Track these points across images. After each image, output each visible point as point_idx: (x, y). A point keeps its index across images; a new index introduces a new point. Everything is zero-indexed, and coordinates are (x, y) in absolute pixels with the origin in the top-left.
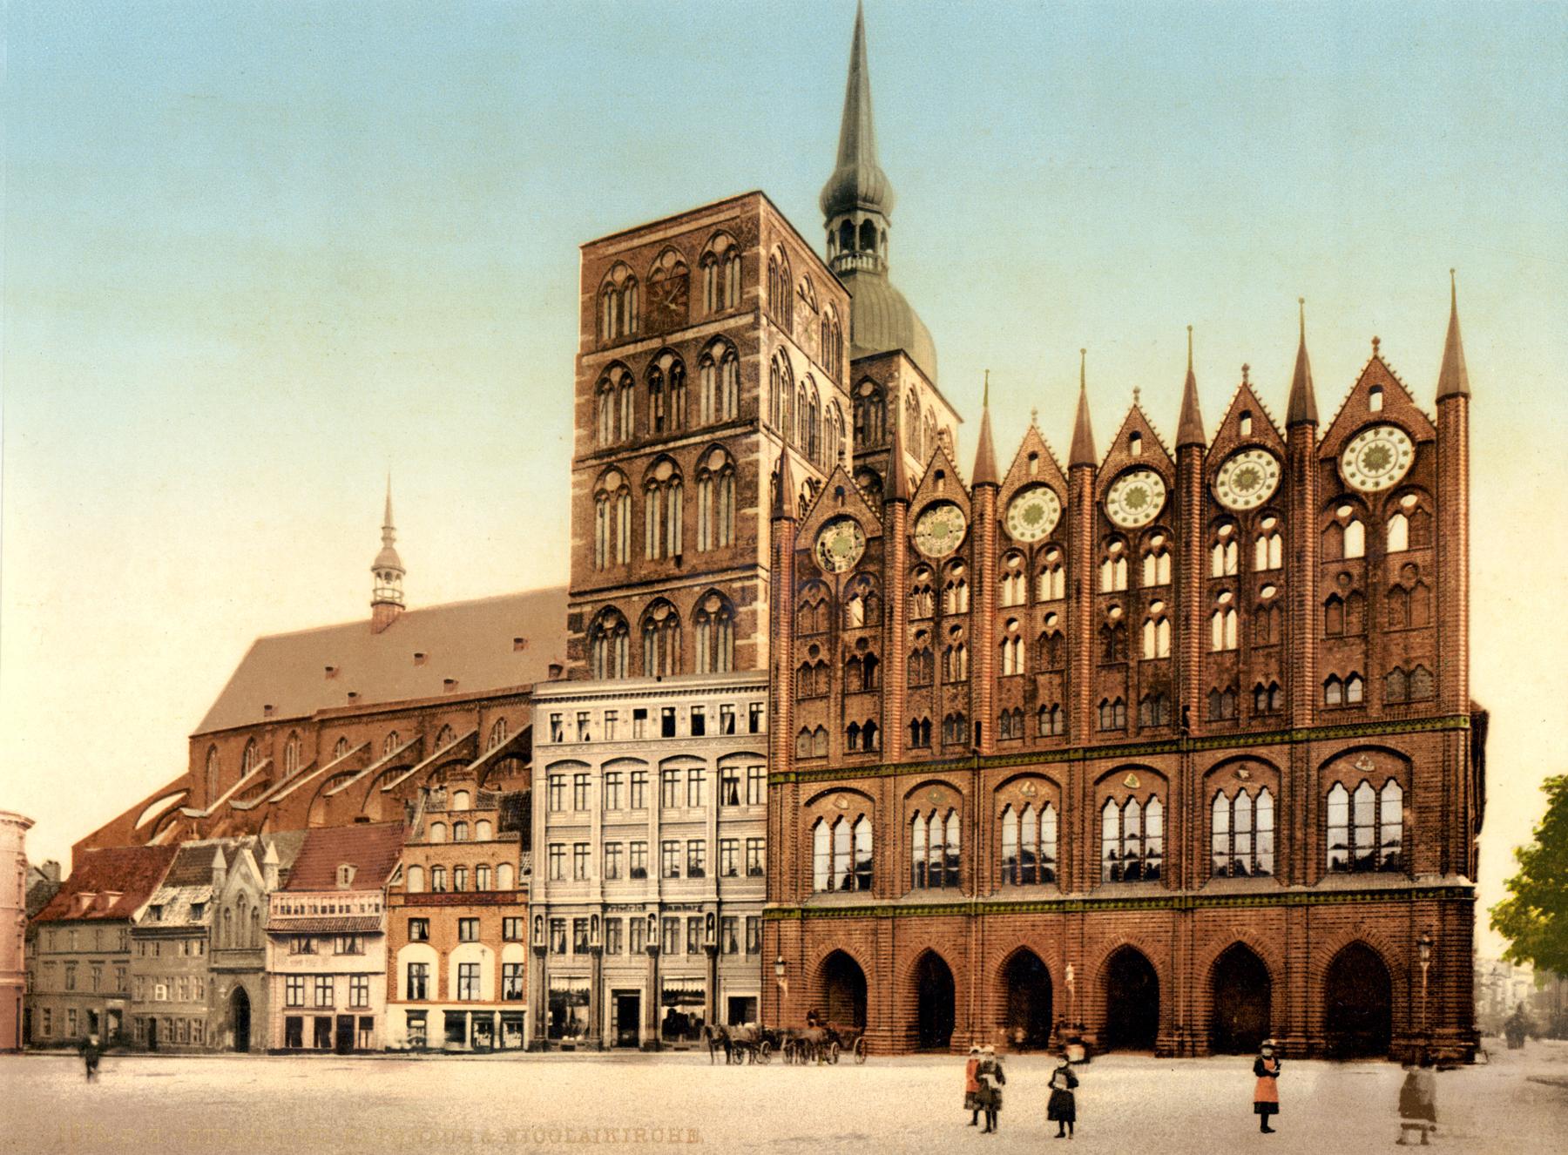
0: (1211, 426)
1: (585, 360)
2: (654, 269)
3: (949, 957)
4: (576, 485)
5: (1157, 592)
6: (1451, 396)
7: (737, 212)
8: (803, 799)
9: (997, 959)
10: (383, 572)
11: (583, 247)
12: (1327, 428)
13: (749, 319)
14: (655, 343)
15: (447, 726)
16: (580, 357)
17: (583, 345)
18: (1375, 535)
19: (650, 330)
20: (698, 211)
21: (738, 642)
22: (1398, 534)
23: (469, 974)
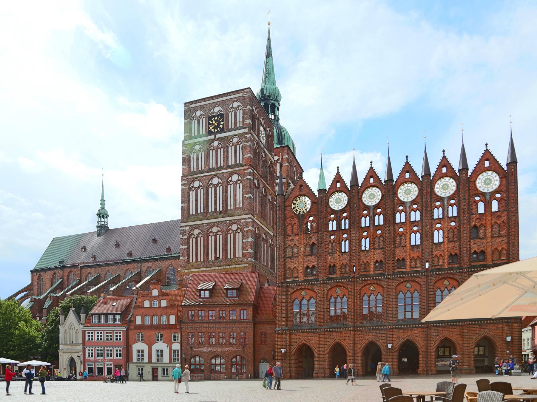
0: (433, 170)
1: (186, 142)
2: (211, 112)
3: (345, 344)
4: (182, 185)
5: (415, 223)
6: (513, 162)
7: (241, 94)
8: (290, 291)
9: (361, 346)
10: (101, 215)
11: (185, 104)
12: (472, 171)
13: (246, 130)
14: (212, 137)
15: (89, 273)
16: (183, 142)
17: (185, 136)
18: (488, 206)
20: (228, 93)
21: (244, 241)
22: (495, 206)
23: (160, 353)
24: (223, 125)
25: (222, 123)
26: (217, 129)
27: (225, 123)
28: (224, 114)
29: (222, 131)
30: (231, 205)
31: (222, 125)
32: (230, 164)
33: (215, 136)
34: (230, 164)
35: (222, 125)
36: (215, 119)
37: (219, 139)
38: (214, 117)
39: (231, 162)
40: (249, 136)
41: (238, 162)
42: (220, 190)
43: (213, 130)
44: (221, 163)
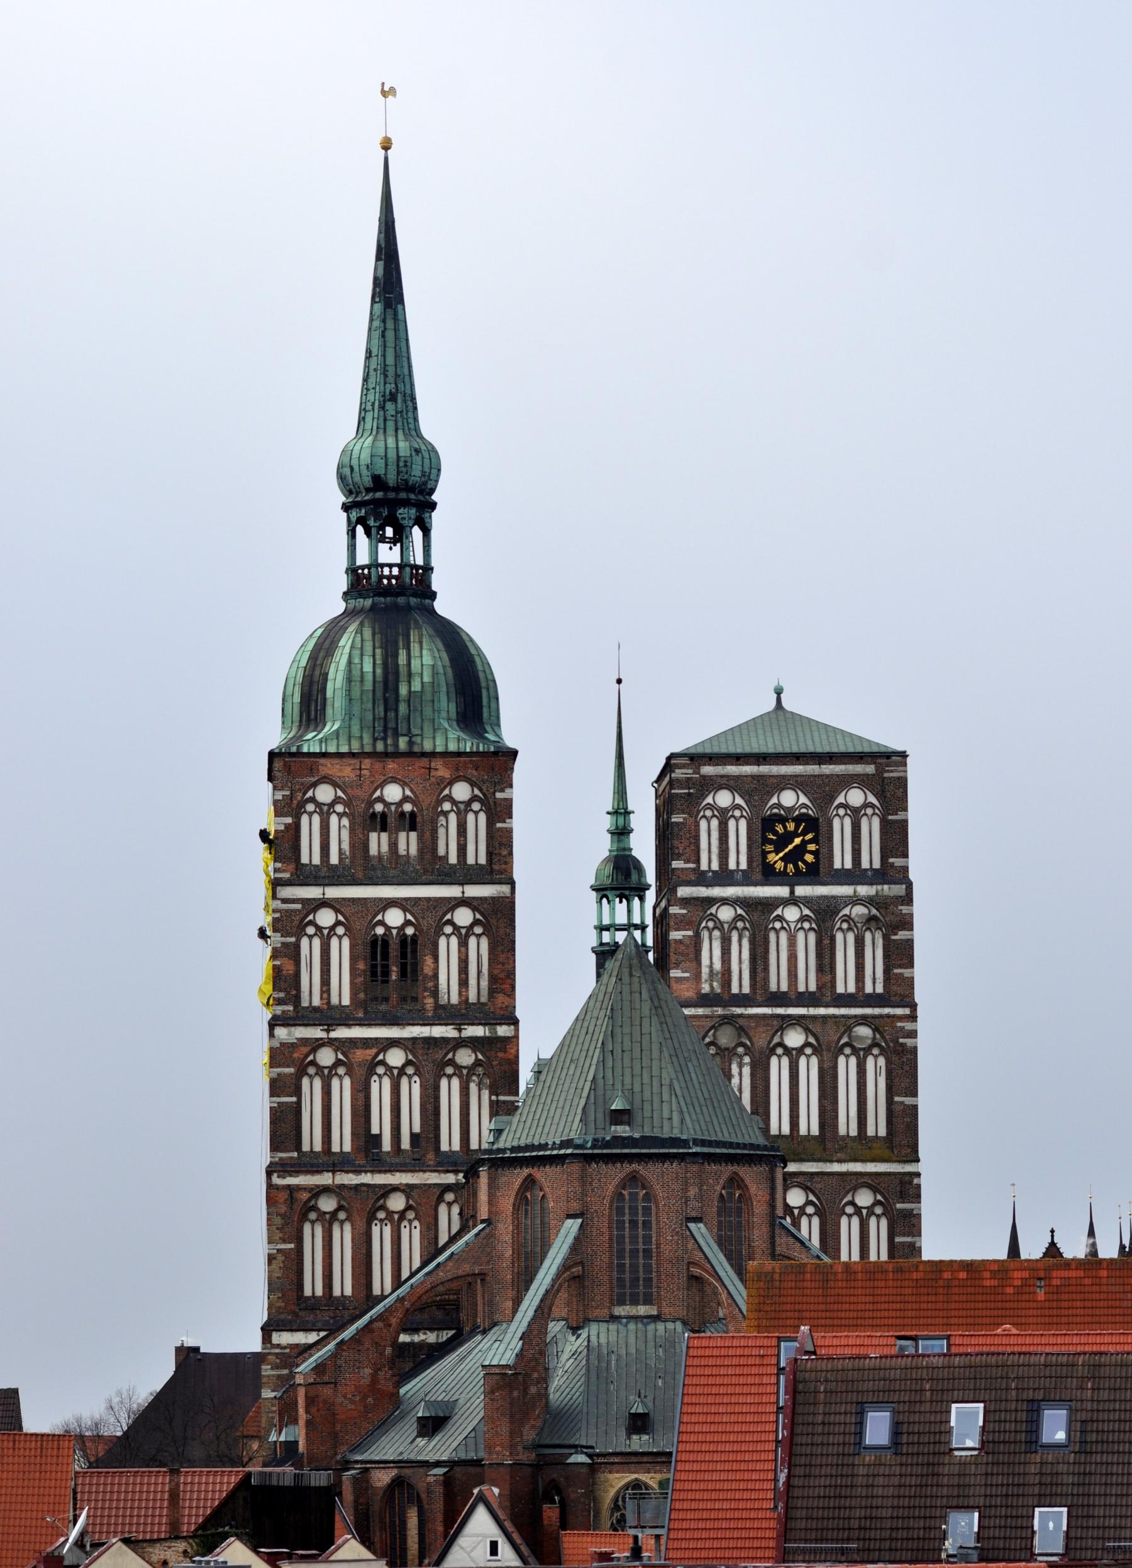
19: (769, 875)
24: (815, 853)
25: (812, 847)
26: (796, 866)
27: (824, 851)
28: (817, 819)
29: (813, 874)
30: (847, 1124)
31: (811, 852)
32: (840, 989)
33: (792, 892)
34: (840, 989)
35: (811, 852)
36: (785, 827)
37: (807, 901)
38: (783, 820)
39: (845, 983)
40: (904, 909)
41: (869, 989)
42: (810, 1069)
43: (780, 866)
44: (808, 981)
